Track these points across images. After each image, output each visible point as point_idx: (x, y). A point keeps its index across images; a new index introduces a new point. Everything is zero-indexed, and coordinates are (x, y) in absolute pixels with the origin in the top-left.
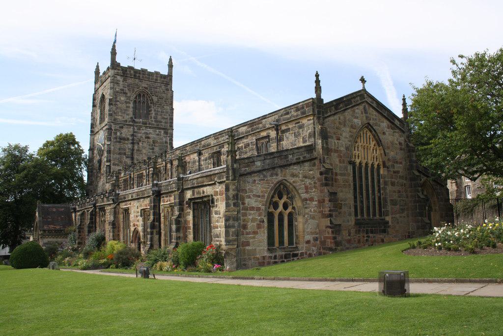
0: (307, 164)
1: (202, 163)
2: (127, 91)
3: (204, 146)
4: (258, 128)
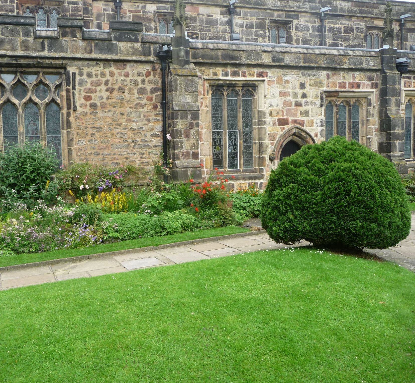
1: (237, 29)
4: (370, 13)
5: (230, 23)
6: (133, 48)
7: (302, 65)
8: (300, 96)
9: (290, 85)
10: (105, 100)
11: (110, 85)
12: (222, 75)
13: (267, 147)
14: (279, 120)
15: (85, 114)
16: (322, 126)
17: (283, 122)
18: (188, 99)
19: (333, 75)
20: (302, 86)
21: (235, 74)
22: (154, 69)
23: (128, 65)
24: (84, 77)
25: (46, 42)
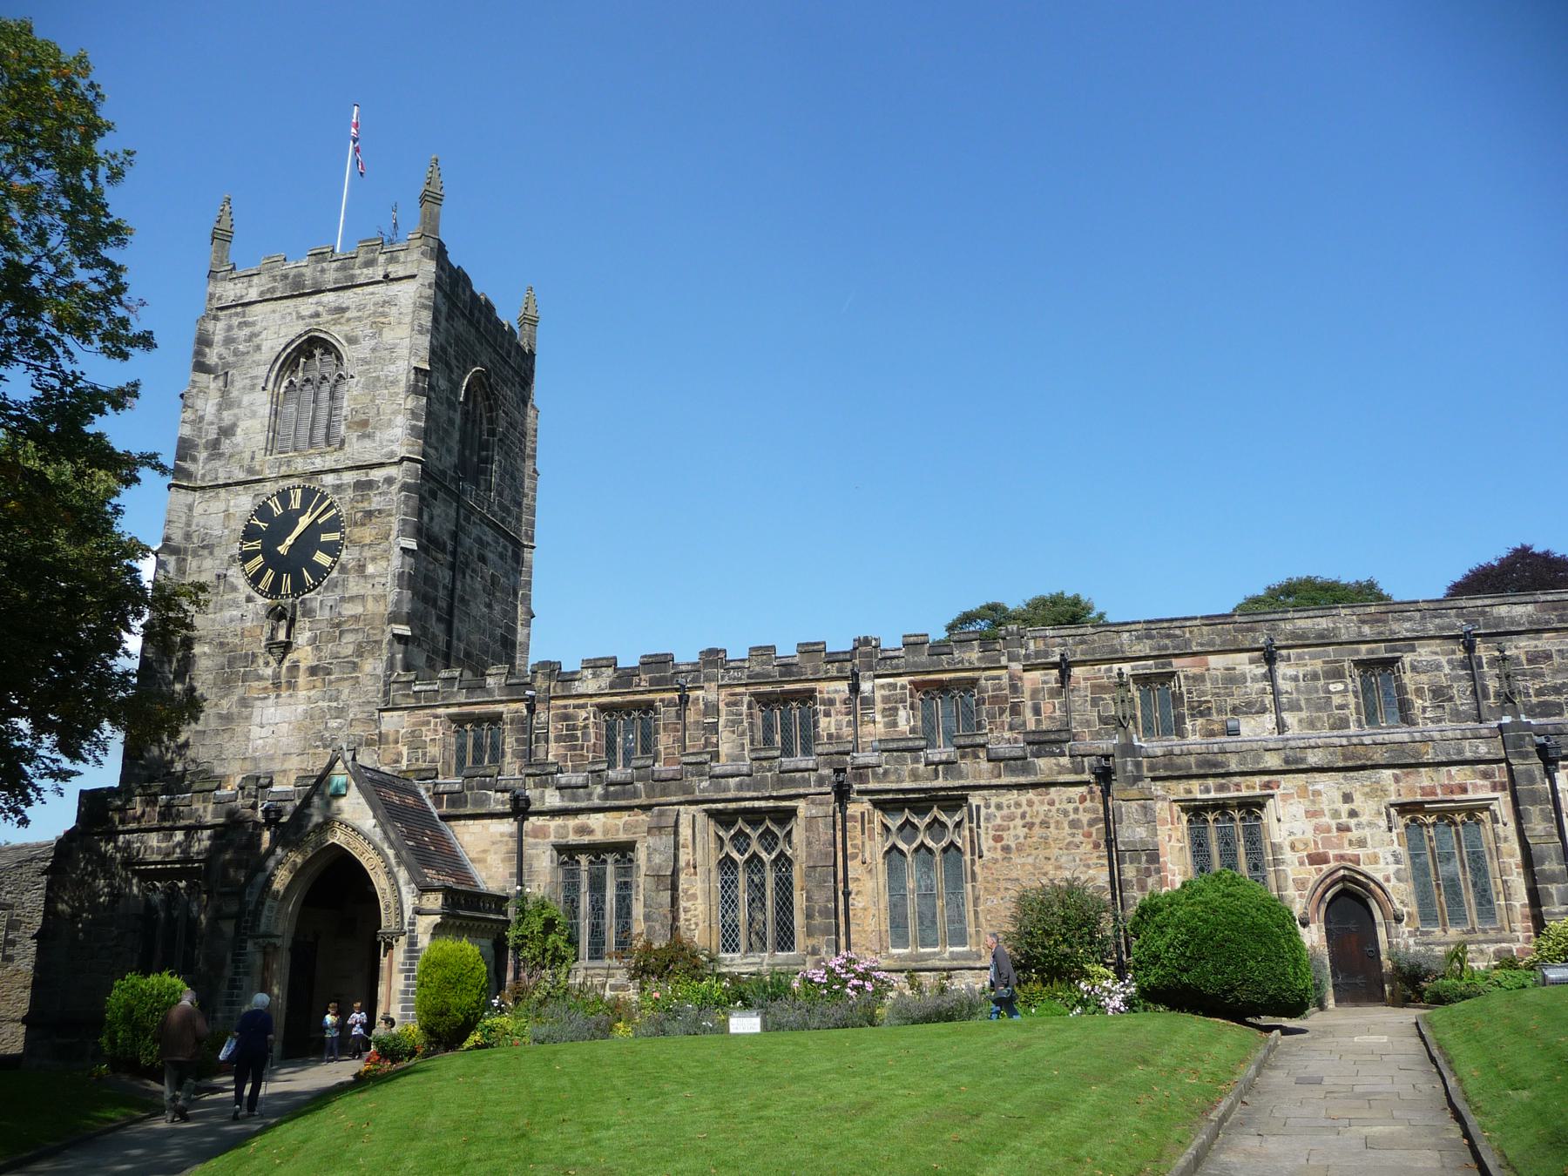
1: (1283, 685)
2: (454, 362)
3: (1294, 635)
5: (1270, 676)
6: (1058, 765)
7: (1341, 764)
8: (1344, 814)
9: (1324, 798)
10: (1021, 840)
11: (1028, 819)
12: (1197, 791)
13: (1292, 901)
14: (1309, 856)
15: (995, 861)
16: (1397, 862)
17: (1317, 859)
18: (1141, 832)
19: (1407, 774)
20: (1347, 798)
21: (1221, 788)
22: (1091, 792)
23: (1053, 790)
24: (992, 809)
25: (940, 768)
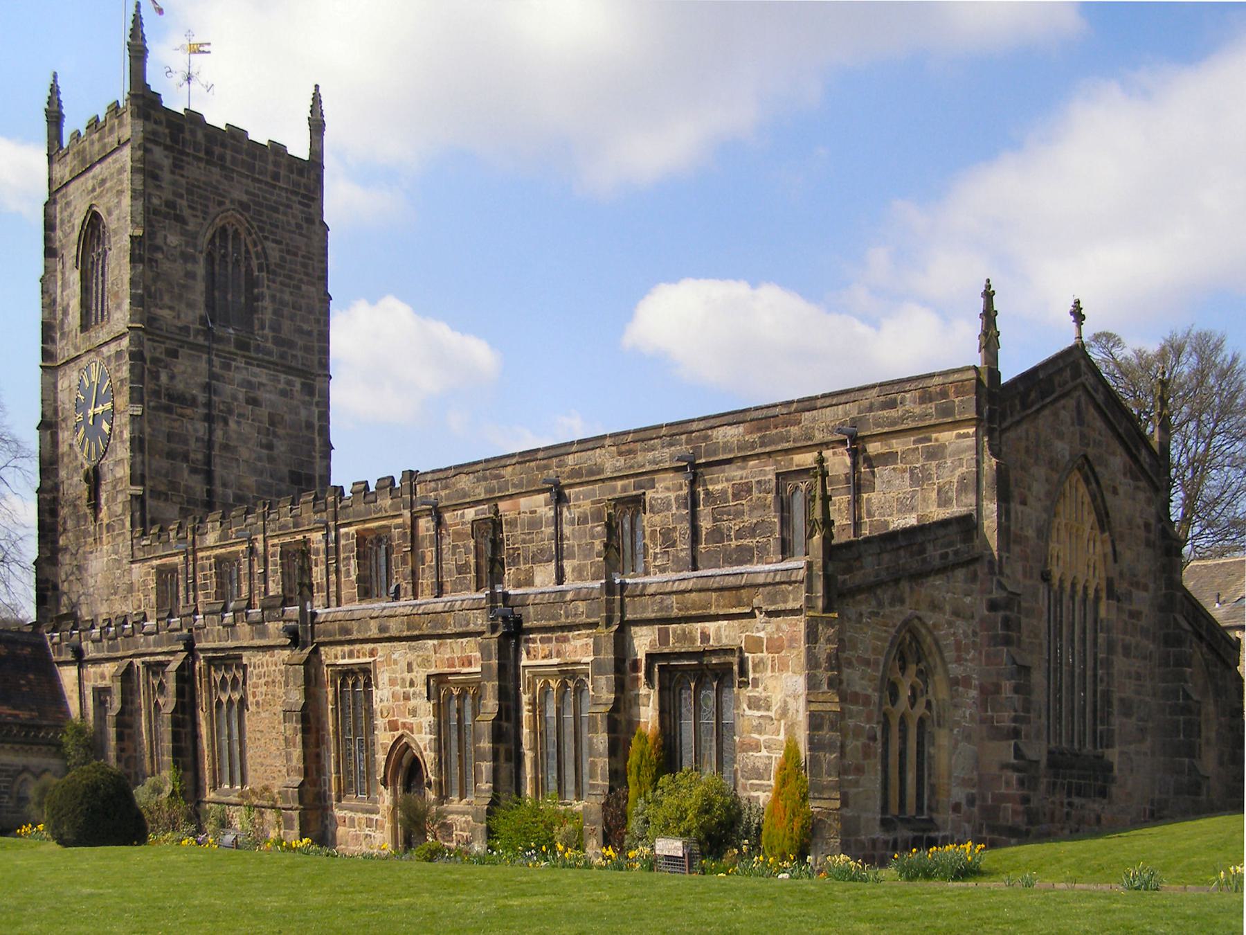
0: (960, 574)
20: (410, 670)
21: (351, 655)
